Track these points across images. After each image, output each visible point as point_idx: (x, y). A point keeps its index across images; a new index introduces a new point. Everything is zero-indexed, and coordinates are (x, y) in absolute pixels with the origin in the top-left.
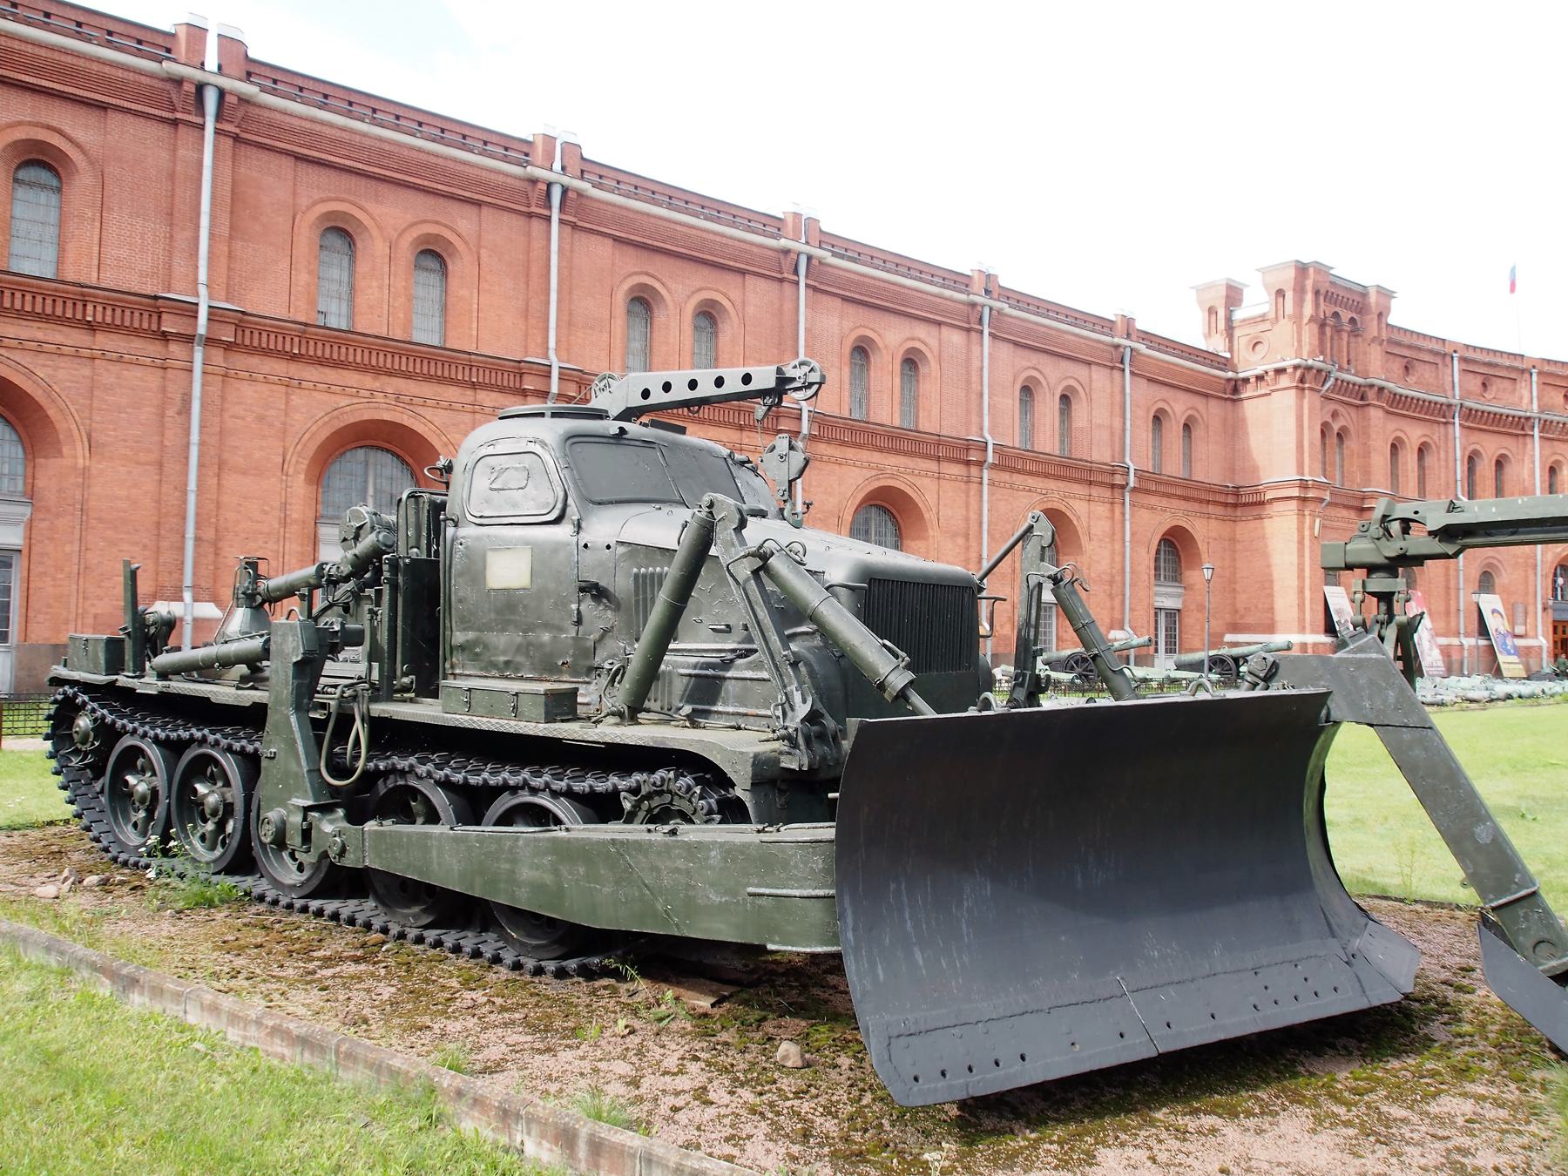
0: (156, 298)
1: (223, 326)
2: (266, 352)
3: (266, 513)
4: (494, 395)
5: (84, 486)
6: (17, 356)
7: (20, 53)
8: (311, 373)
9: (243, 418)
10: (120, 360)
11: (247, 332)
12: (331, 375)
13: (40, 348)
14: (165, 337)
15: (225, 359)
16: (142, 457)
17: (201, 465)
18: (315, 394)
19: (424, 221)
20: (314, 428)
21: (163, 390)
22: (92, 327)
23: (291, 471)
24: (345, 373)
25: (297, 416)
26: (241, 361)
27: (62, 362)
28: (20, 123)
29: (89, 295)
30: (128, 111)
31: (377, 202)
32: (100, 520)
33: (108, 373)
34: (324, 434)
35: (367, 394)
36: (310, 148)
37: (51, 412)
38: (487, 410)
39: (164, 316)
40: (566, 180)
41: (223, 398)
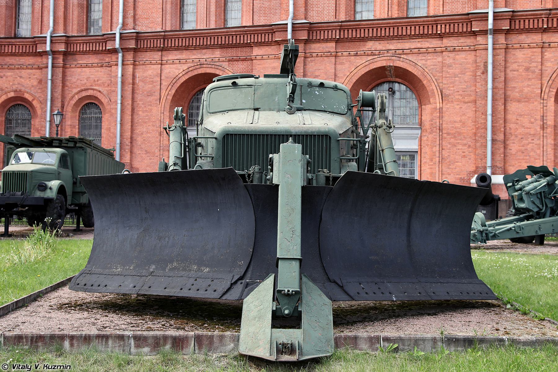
0: (468, 14)
1: (502, 21)
2: (529, 31)
3: (532, 123)
5: (441, 117)
6: (410, 57)
9: (518, 71)
10: (454, 50)
11: (517, 22)
13: (419, 52)
14: (474, 34)
15: (506, 39)
16: (467, 99)
17: (494, 99)
21: (476, 62)
22: (441, 36)
23: (546, 97)
26: (515, 39)
27: (429, 57)
29: (438, 20)
32: (448, 134)
33: (449, 58)
37: (425, 82)
39: (473, 23)
41: (506, 61)
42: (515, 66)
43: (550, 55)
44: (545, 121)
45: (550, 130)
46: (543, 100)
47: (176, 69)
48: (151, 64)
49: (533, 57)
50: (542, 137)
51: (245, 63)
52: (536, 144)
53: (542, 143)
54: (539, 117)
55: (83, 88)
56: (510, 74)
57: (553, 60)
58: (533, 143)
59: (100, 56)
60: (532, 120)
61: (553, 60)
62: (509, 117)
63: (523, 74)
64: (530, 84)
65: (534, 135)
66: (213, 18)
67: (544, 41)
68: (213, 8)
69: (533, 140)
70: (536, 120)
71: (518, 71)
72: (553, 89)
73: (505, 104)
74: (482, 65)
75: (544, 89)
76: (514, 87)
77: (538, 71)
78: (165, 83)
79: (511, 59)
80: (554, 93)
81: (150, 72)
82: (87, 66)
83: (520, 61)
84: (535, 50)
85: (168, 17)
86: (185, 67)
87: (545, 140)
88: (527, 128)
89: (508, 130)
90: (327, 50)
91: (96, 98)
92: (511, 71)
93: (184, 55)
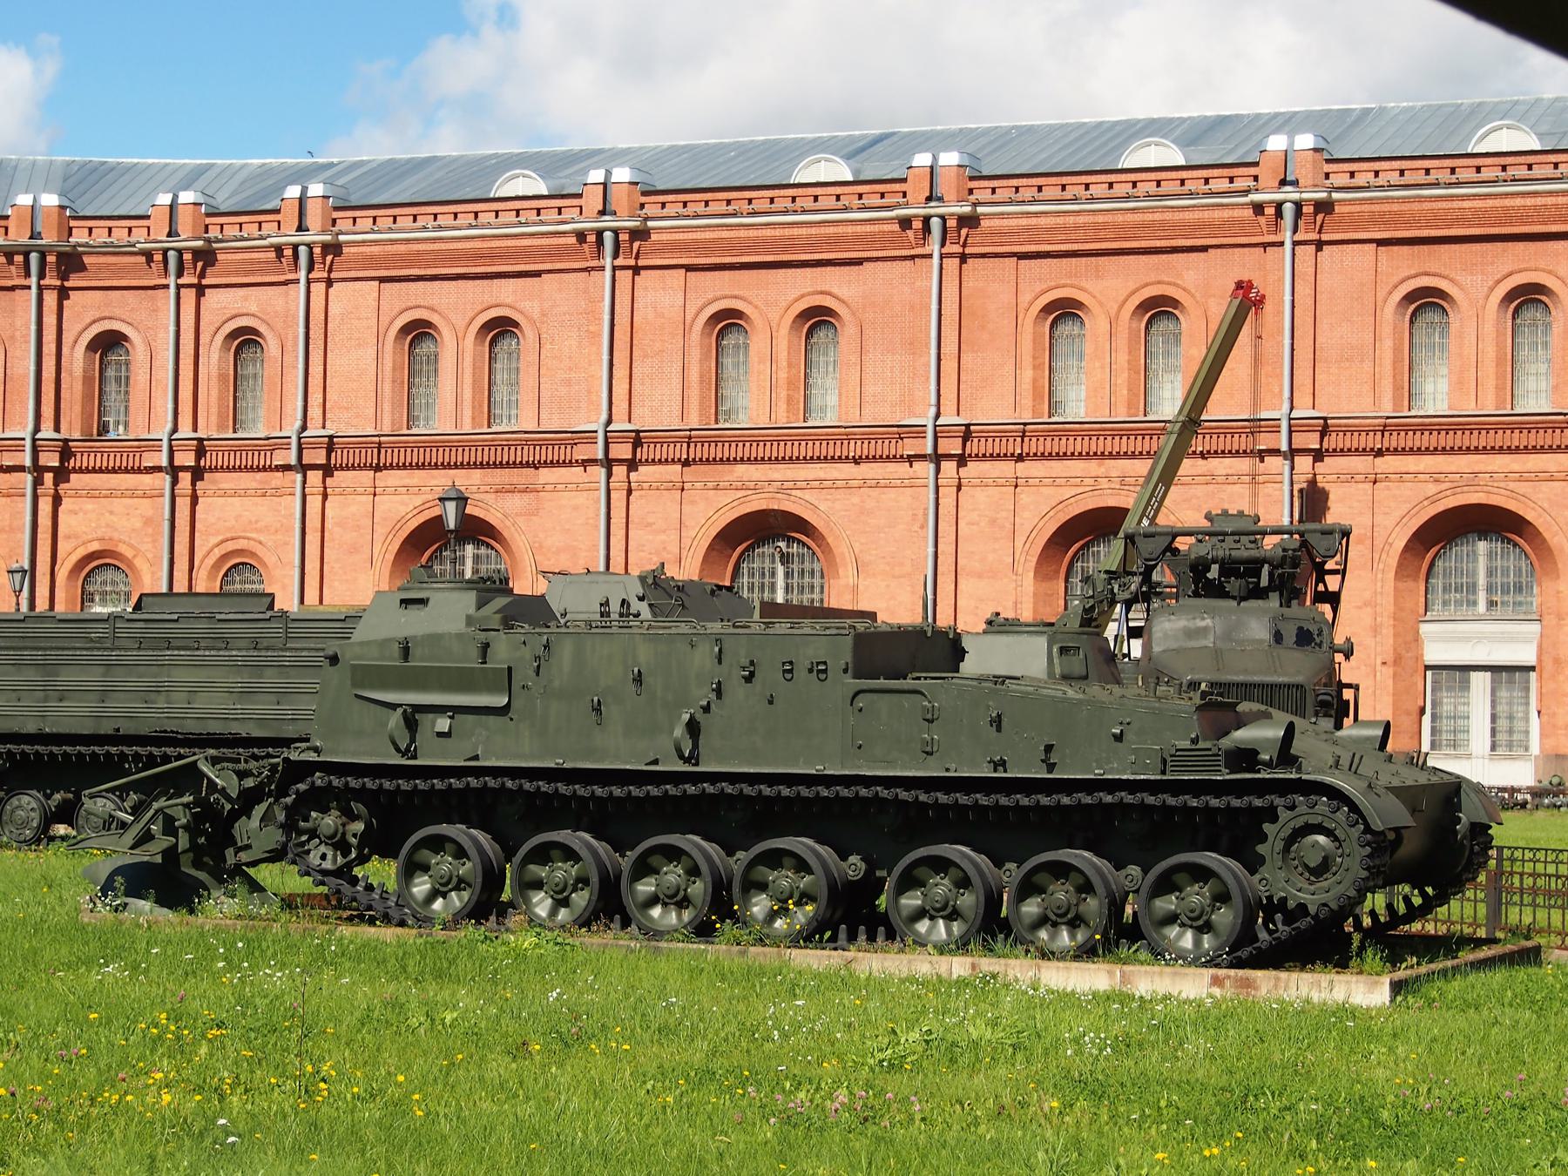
2: (995, 457)
6: (807, 495)
7: (799, 237)
12: (1057, 467)
13: (821, 485)
18: (1043, 489)
19: (1146, 285)
22: (857, 461)
25: (1027, 514)
27: (839, 494)
28: (803, 296)
30: (877, 259)
31: (1097, 277)
36: (1030, 242)
38: (1219, 479)
40: (1296, 196)
47: (403, 503)
48: (355, 493)
51: (526, 496)
55: (229, 535)
59: (259, 475)
66: (467, 413)
68: (467, 394)
74: (920, 516)
78: (381, 531)
81: (353, 509)
82: (235, 494)
85: (387, 407)
86: (418, 501)
90: (668, 478)
91: (253, 554)
93: (417, 477)
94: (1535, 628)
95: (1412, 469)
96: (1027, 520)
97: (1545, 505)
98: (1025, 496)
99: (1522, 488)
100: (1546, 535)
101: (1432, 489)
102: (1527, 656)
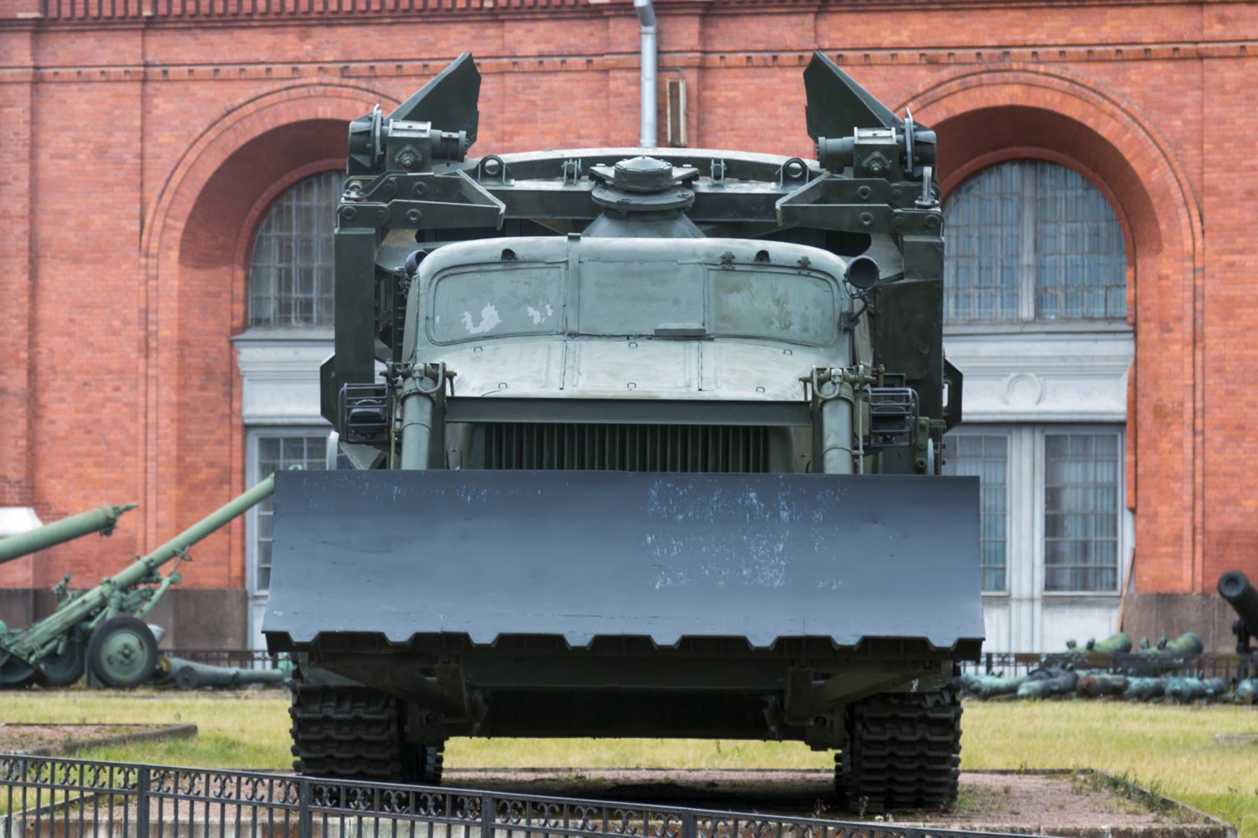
3: (115, 332)
4: (542, 28)
8: (183, 49)
9: (73, 156)
15: (35, 48)
18: (196, 88)
20: (192, 157)
24: (245, 35)
26: (65, 50)
34: (212, 163)
35: (285, 70)
38: (527, 64)
41: (34, 120)
42: (64, 141)
43: (170, 107)
44: (152, 328)
45: (165, 357)
46: (147, 255)
49: (117, 112)
50: (142, 382)
52: (126, 405)
53: (141, 399)
54: (133, 314)
56: (51, 168)
57: (176, 123)
58: (118, 400)
60: (116, 323)
61: (176, 123)
62: (47, 311)
63: (90, 167)
64: (109, 201)
65: (121, 372)
67: (150, 58)
69: (117, 389)
70: (126, 322)
71: (73, 156)
72: (176, 219)
73: (33, 271)
75: (148, 221)
76: (64, 213)
77: (131, 160)
79: (51, 116)
80: (178, 235)
83: (81, 124)
84: (122, 88)
87: (152, 389)
88: (102, 350)
89: (44, 360)
92: (53, 157)
94: (1122, 348)
95: (888, 39)
96: (167, 143)
97: (1136, 109)
98: (163, 104)
99: (1093, 75)
100: (1138, 167)
101: (924, 78)
102: (1108, 401)
